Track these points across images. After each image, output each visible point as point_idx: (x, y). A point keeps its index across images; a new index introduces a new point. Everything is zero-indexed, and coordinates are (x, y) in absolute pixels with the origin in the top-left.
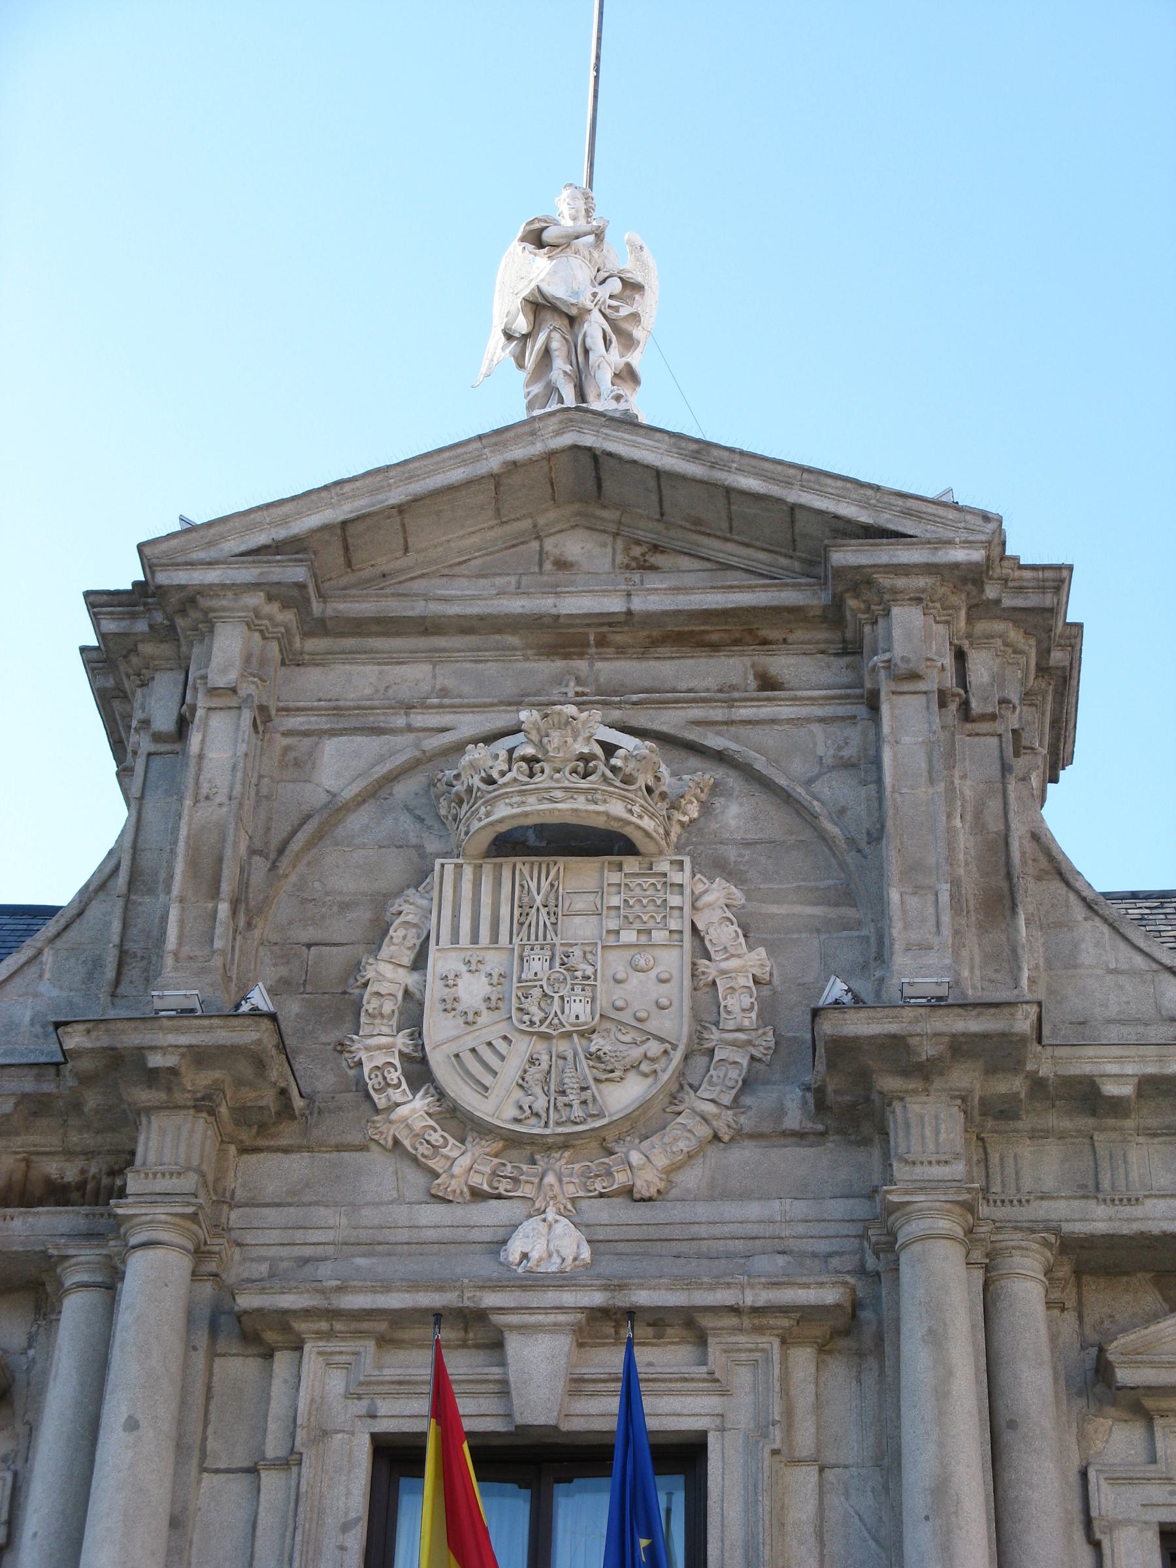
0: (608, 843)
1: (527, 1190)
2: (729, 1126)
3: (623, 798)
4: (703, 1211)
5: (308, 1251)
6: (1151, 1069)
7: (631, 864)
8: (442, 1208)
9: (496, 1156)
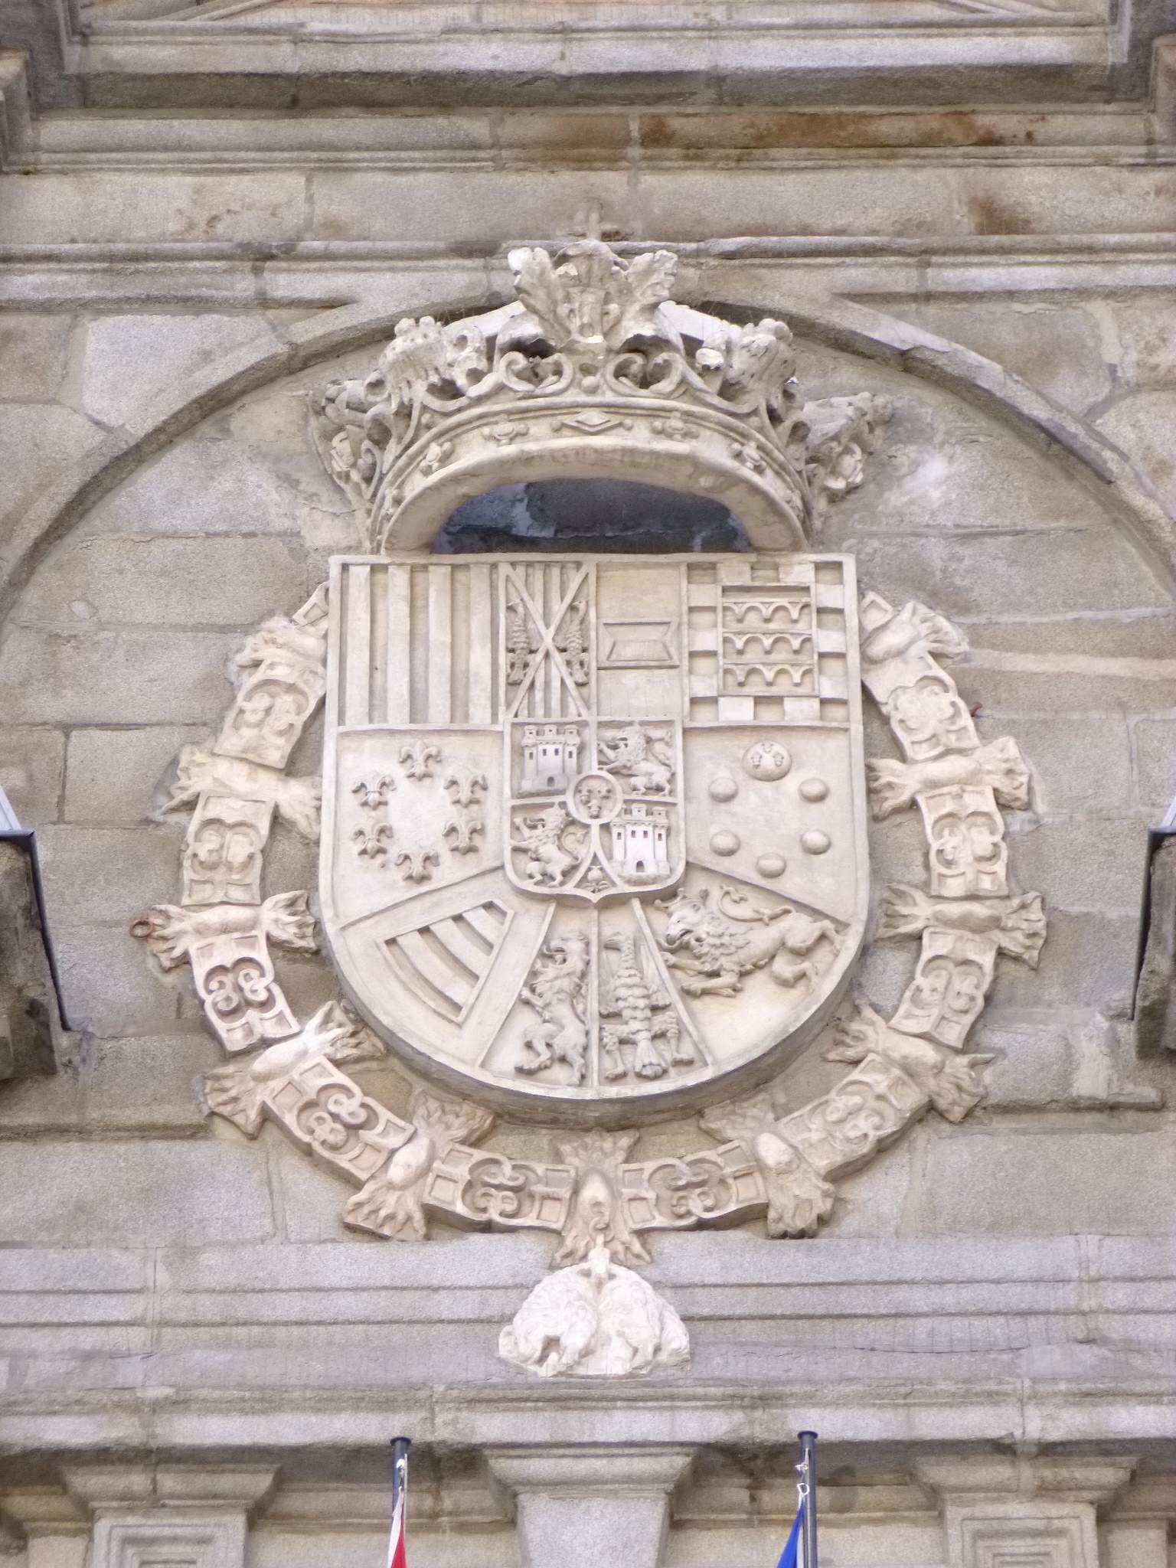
1: (553, 1216)
2: (959, 1088)
3: (729, 432)
4: (915, 1258)
5: (88, 1340)
7: (734, 568)
8: (367, 1250)
9: (476, 1142)
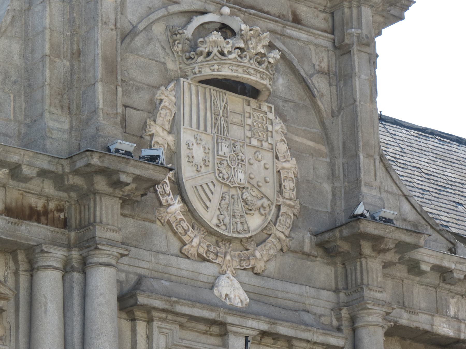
0: (249, 91)
2: (287, 246)
6: (438, 262)
